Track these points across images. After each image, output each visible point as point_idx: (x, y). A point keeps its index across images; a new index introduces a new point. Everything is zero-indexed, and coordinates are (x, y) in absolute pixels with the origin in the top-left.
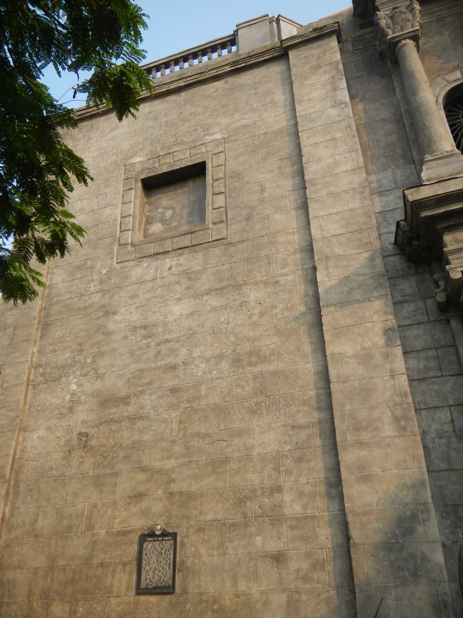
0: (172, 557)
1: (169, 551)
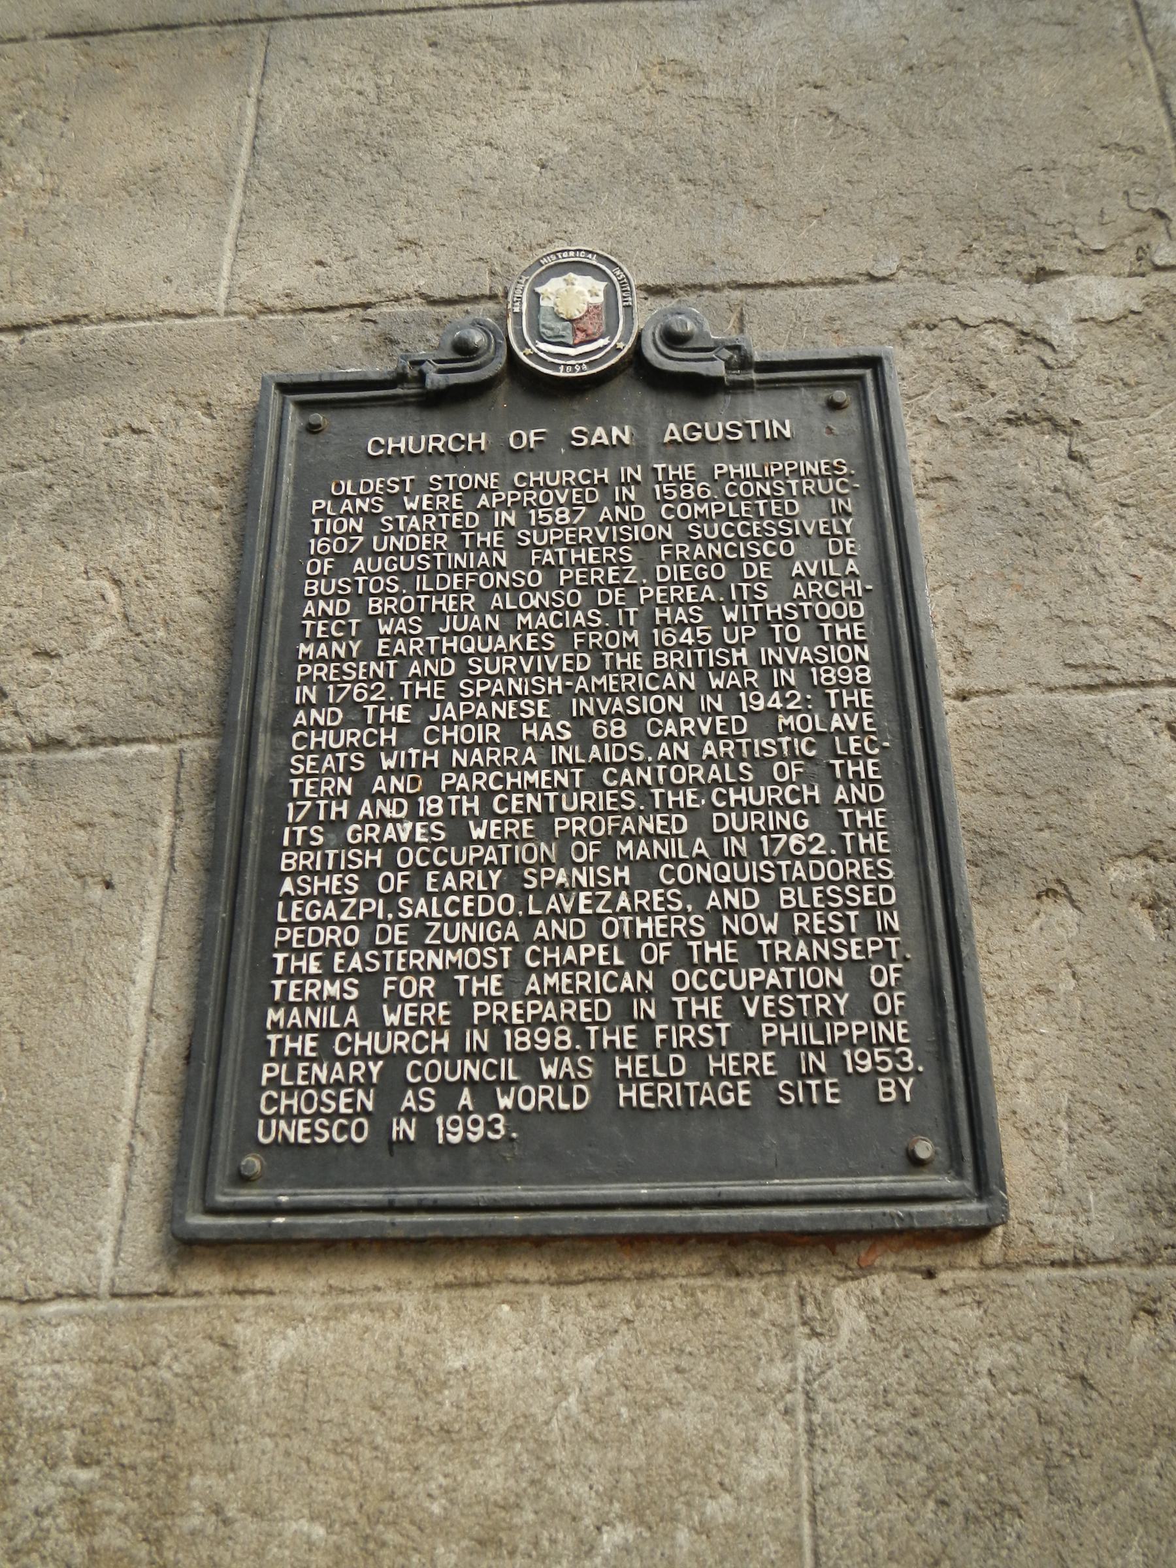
0: (853, 667)
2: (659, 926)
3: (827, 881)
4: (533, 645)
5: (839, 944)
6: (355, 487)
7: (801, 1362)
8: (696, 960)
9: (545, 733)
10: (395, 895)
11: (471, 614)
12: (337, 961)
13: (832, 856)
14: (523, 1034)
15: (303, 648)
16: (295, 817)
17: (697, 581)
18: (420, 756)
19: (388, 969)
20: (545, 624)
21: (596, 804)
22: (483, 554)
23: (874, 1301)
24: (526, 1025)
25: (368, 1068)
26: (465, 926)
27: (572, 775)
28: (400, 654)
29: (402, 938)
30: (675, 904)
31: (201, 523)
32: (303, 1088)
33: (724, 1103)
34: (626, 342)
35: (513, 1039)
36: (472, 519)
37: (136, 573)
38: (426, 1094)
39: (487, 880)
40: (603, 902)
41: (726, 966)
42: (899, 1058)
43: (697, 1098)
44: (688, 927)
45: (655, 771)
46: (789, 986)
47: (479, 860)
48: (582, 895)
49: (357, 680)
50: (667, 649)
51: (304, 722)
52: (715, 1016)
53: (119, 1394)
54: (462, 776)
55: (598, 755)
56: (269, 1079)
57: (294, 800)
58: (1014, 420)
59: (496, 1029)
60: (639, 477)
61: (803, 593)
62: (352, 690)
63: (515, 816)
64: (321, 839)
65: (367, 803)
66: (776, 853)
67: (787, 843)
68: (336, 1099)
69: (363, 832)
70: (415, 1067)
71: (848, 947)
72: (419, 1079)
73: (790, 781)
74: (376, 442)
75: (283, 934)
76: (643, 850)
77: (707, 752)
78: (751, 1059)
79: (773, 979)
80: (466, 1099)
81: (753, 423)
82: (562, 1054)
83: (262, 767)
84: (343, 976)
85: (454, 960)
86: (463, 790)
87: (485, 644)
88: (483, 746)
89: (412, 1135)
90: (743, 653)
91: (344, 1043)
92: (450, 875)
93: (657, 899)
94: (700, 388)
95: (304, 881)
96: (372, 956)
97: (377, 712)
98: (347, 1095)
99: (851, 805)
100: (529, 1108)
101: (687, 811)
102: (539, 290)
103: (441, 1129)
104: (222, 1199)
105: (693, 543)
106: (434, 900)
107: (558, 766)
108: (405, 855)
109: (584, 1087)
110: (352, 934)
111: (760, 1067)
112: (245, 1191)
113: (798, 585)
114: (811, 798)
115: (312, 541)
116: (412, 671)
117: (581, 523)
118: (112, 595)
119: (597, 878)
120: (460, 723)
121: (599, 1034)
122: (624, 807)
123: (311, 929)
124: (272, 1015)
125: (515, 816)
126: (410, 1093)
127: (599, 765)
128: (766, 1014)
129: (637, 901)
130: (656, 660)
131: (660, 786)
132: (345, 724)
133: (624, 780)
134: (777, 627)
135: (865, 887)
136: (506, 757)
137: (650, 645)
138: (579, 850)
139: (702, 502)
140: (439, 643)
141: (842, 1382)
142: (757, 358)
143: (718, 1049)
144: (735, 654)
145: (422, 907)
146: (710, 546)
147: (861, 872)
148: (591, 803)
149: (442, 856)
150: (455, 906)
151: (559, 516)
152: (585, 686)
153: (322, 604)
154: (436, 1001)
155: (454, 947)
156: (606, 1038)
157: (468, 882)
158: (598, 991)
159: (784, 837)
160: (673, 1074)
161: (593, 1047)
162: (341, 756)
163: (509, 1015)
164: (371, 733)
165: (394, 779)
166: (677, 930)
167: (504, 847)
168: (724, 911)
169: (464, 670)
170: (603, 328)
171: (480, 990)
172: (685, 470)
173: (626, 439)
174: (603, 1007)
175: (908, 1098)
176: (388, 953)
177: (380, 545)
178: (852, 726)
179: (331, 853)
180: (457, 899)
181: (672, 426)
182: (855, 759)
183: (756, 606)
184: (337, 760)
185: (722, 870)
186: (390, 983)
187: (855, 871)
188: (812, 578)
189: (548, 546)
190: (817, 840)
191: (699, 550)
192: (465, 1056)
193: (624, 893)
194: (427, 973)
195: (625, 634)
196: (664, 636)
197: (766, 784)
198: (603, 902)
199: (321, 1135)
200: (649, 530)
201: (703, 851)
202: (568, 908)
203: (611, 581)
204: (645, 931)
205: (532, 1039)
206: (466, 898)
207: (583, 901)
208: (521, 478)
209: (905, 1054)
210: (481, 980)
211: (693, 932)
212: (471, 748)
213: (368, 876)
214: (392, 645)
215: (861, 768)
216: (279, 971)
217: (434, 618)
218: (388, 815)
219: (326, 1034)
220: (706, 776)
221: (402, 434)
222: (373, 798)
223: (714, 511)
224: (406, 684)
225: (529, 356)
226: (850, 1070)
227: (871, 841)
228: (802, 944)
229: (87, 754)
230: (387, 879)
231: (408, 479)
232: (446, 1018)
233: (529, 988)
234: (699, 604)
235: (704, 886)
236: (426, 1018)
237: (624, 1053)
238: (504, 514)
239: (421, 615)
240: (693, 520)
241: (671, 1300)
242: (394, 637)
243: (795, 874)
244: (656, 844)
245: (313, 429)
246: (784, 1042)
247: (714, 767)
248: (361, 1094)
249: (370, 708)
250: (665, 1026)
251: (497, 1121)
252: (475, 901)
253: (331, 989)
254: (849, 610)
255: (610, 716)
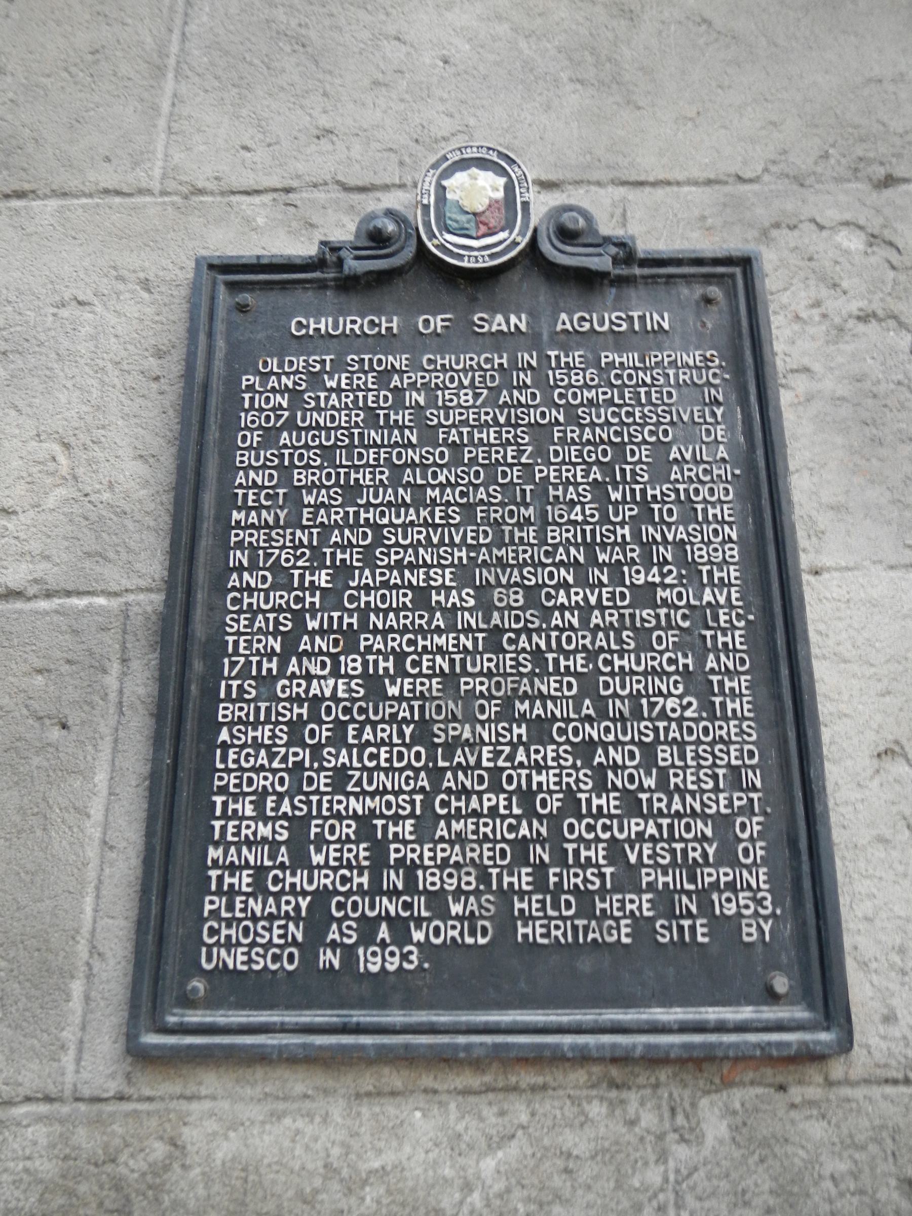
1: (661, 469)
2: (553, 779)
3: (699, 742)
4: (441, 518)
5: (709, 799)
6: (281, 365)
7: (671, 1164)
8: (584, 811)
9: (451, 600)
10: (319, 747)
11: (385, 487)
12: (270, 804)
13: (703, 719)
14: (433, 874)
15: (236, 515)
16: (230, 671)
17: (585, 462)
18: (341, 618)
19: (314, 813)
20: (451, 498)
21: (497, 666)
22: (396, 432)
23: (735, 1113)
24: (436, 866)
25: (297, 904)
26: (382, 775)
27: (475, 640)
28: (322, 523)
29: (326, 785)
30: (566, 760)
31: (142, 392)
32: (240, 920)
33: (608, 939)
34: (524, 236)
35: (425, 880)
36: (386, 397)
37: (84, 438)
38: (349, 927)
39: (401, 734)
40: (503, 756)
41: (611, 817)
42: (760, 902)
43: (585, 935)
44: (577, 781)
45: (548, 638)
46: (665, 836)
47: (394, 716)
48: (485, 749)
49: (284, 547)
50: (560, 525)
51: (237, 584)
52: (602, 861)
53: (83, 1188)
54: (379, 637)
55: (499, 622)
56: (211, 912)
57: (230, 656)
58: (864, 318)
59: (410, 870)
60: (534, 363)
61: (679, 476)
62: (279, 556)
63: (426, 676)
64: (254, 692)
65: (294, 660)
66: (654, 714)
67: (664, 707)
68: (270, 930)
69: (291, 687)
70: (339, 903)
71: (717, 802)
72: (342, 913)
73: (667, 650)
74: (299, 323)
75: (221, 779)
76: (538, 711)
77: (594, 621)
78: (632, 901)
79: (652, 830)
80: (384, 932)
81: (635, 314)
82: (467, 894)
83: (199, 630)
84: (275, 819)
85: (372, 806)
86: (379, 651)
87: (398, 516)
88: (397, 611)
89: (336, 964)
90: (627, 530)
91: (276, 881)
92: (368, 729)
93: (551, 755)
94: (587, 281)
95: (239, 731)
96: (300, 801)
97: (302, 576)
98: (279, 927)
99: (720, 673)
100: (438, 941)
101: (576, 674)
102: (445, 183)
103: (362, 959)
104: (172, 1020)
105: (582, 427)
106: (355, 750)
107: (464, 631)
108: (328, 710)
109: (487, 923)
110: (282, 781)
111: (640, 908)
112: (191, 1012)
113: (675, 468)
114: (686, 666)
115: (243, 415)
116: (333, 539)
117: (483, 405)
118: (62, 459)
119: (498, 734)
120: (377, 589)
121: (500, 877)
122: (521, 669)
123: (246, 775)
124: (214, 853)
125: (426, 676)
126: (334, 926)
127: (498, 631)
128: (646, 860)
129: (533, 756)
130: (550, 534)
131: (552, 651)
132: (274, 587)
133: (521, 645)
134: (656, 507)
135: (732, 748)
136: (417, 621)
137: (544, 522)
138: (482, 709)
139: (589, 388)
140: (356, 514)
141: (706, 1183)
142: (641, 255)
143: (603, 892)
144: (619, 531)
145: (344, 758)
146: (598, 430)
147: (728, 734)
148: (492, 665)
149: (361, 710)
150: (372, 757)
151: (463, 398)
152: (487, 557)
153: (252, 474)
154: (357, 842)
155: (372, 795)
156: (506, 879)
157: (385, 735)
158: (499, 837)
159: (661, 700)
160: (564, 913)
161: (494, 887)
162: (271, 616)
163: (421, 857)
164: (297, 597)
165: (318, 639)
166: (568, 784)
167: (416, 704)
168: (609, 766)
169: (379, 540)
170: (503, 222)
171: (396, 834)
172: (576, 357)
173: (523, 327)
174: (503, 852)
175: (767, 938)
176: (314, 798)
177: (304, 420)
178: (722, 600)
179: (263, 705)
180: (374, 750)
181: (564, 316)
182: (724, 632)
183: (637, 487)
184: (267, 620)
185: (607, 730)
186: (317, 826)
187: (724, 733)
188: (687, 462)
189: (454, 425)
190: (690, 704)
191: (587, 435)
192: (382, 893)
193: (521, 748)
194: (348, 817)
195: (522, 509)
196: (557, 513)
197: (646, 651)
198: (503, 756)
199: (257, 963)
200: (543, 414)
201: (591, 712)
202: (472, 761)
203: (510, 460)
204: (540, 784)
205: (441, 879)
206: (383, 749)
207: (485, 755)
208: (430, 361)
209: (765, 898)
210: (396, 824)
211: (581, 785)
212: (386, 612)
213: (295, 727)
214: (315, 514)
215: (729, 639)
216: (218, 813)
217: (352, 491)
218: (313, 672)
219: (260, 872)
220: (593, 643)
221: (322, 315)
222: (300, 656)
223: (601, 397)
224: (328, 551)
225: (437, 247)
226: (718, 912)
227: (737, 705)
228: (676, 798)
229: (43, 605)
230: (312, 731)
231: (328, 358)
232: (365, 858)
233: (439, 833)
234: (588, 484)
235: (590, 745)
236: (348, 859)
237: (522, 894)
238: (414, 394)
239: (341, 487)
240: (582, 404)
241: (561, 1108)
242: (317, 507)
243: (671, 735)
244: (550, 704)
245: (242, 308)
246: (660, 887)
247: (601, 635)
248: (291, 926)
249: (296, 573)
250: (558, 870)
251: (411, 952)
252: (390, 752)
253: (265, 831)
254: (719, 493)
255: (509, 586)
